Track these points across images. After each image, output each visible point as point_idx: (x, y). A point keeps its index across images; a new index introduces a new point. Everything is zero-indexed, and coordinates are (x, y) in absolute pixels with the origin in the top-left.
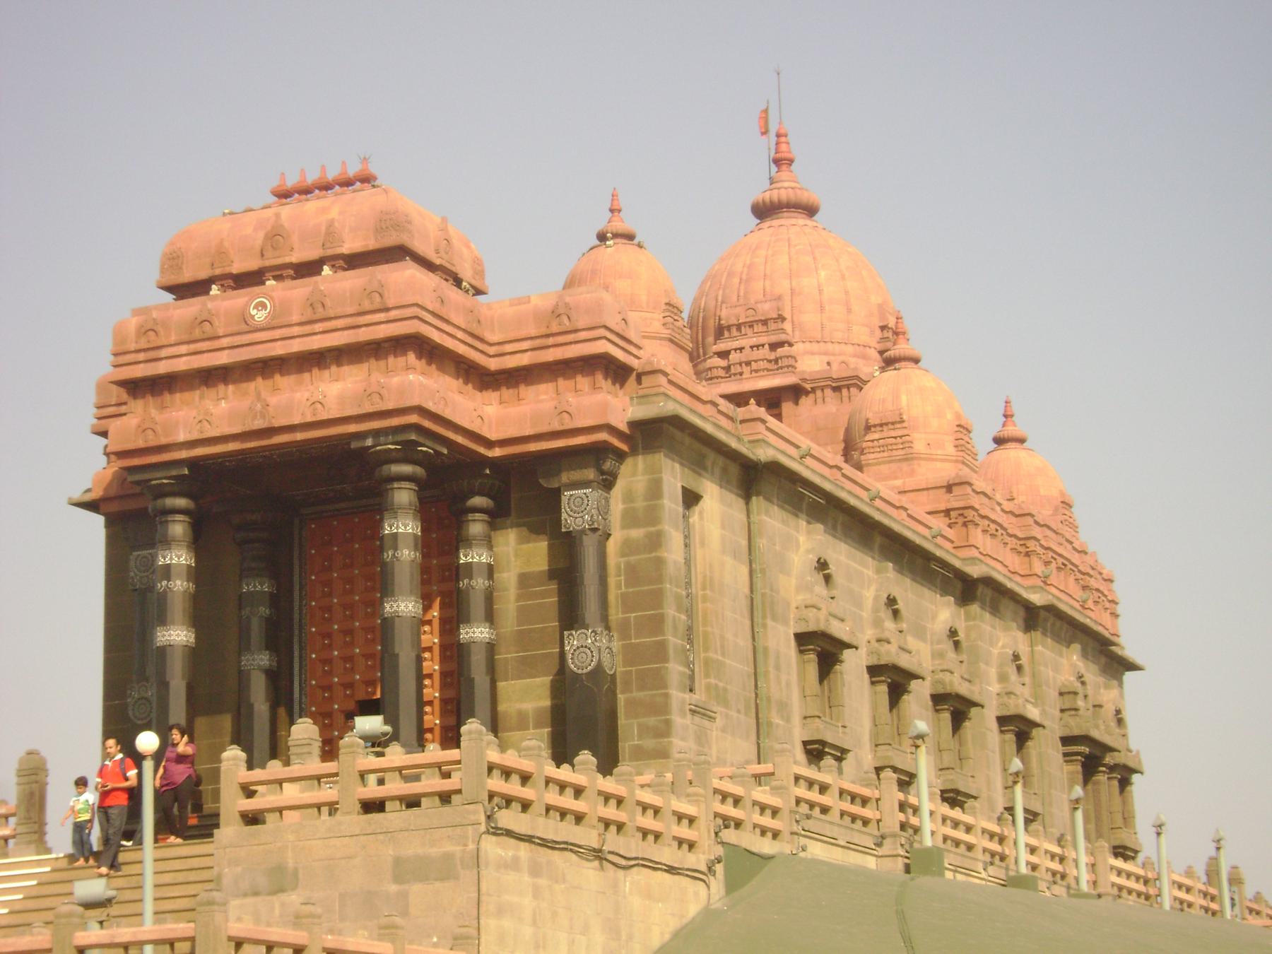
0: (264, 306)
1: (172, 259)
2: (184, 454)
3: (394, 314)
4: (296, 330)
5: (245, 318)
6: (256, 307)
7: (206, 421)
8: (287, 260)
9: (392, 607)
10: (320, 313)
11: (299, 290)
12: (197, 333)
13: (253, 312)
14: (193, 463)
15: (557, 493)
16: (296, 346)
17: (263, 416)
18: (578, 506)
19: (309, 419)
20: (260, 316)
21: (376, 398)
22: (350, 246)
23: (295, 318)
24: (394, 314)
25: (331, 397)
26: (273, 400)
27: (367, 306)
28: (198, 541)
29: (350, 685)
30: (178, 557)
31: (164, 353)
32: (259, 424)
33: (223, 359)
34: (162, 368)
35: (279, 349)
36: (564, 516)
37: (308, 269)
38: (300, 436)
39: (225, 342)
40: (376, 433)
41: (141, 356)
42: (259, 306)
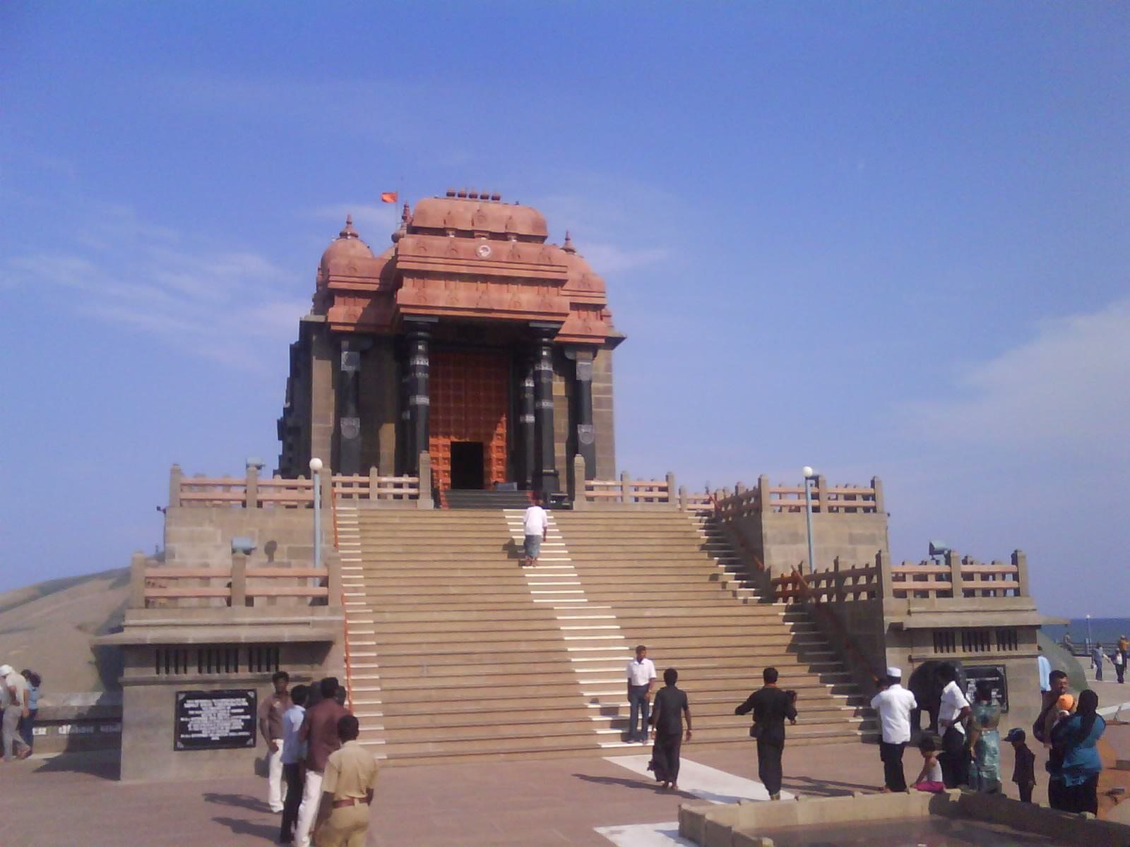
2: (440, 312)
3: (554, 269)
5: (476, 253)
6: (484, 249)
8: (489, 230)
11: (505, 247)
13: (481, 251)
15: (574, 363)
16: (505, 273)
19: (512, 309)
20: (484, 254)
24: (554, 269)
25: (524, 301)
28: (429, 354)
30: (422, 362)
33: (464, 270)
34: (429, 267)
35: (495, 272)
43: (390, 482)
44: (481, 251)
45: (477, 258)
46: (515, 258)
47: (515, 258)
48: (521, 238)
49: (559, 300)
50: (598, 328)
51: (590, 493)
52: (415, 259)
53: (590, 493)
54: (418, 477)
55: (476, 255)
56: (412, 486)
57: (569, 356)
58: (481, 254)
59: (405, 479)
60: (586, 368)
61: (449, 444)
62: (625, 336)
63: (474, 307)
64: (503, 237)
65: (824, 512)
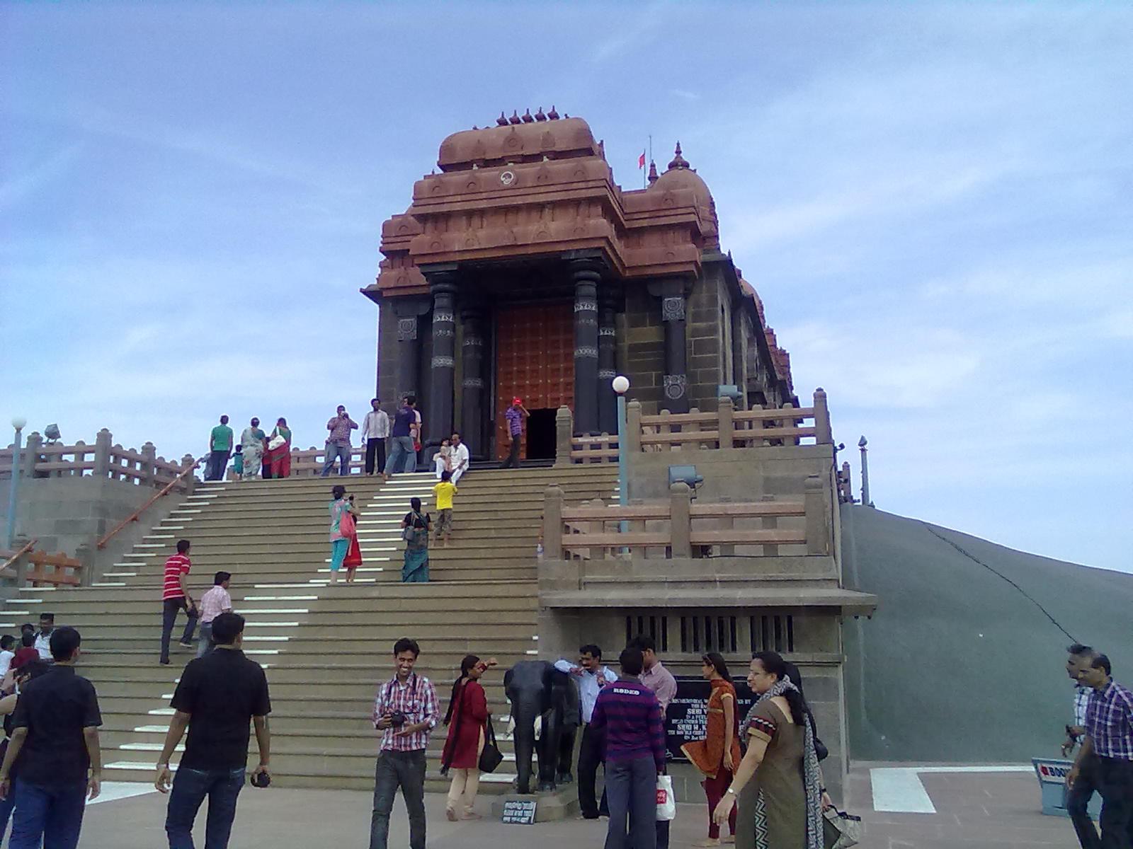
0: (510, 177)
1: (446, 149)
2: (458, 257)
3: (591, 184)
4: (532, 190)
7: (468, 240)
11: (530, 169)
13: (503, 179)
14: (462, 264)
15: (660, 299)
18: (673, 306)
22: (560, 146)
23: (530, 184)
24: (591, 184)
34: (445, 208)
37: (536, 158)
38: (530, 251)
39: (484, 195)
41: (432, 201)
42: (506, 176)
46: (543, 179)
47: (543, 179)
48: (557, 155)
51: (578, 454)
52: (432, 201)
53: (578, 454)
55: (498, 185)
57: (654, 290)
64: (536, 158)
65: (727, 451)
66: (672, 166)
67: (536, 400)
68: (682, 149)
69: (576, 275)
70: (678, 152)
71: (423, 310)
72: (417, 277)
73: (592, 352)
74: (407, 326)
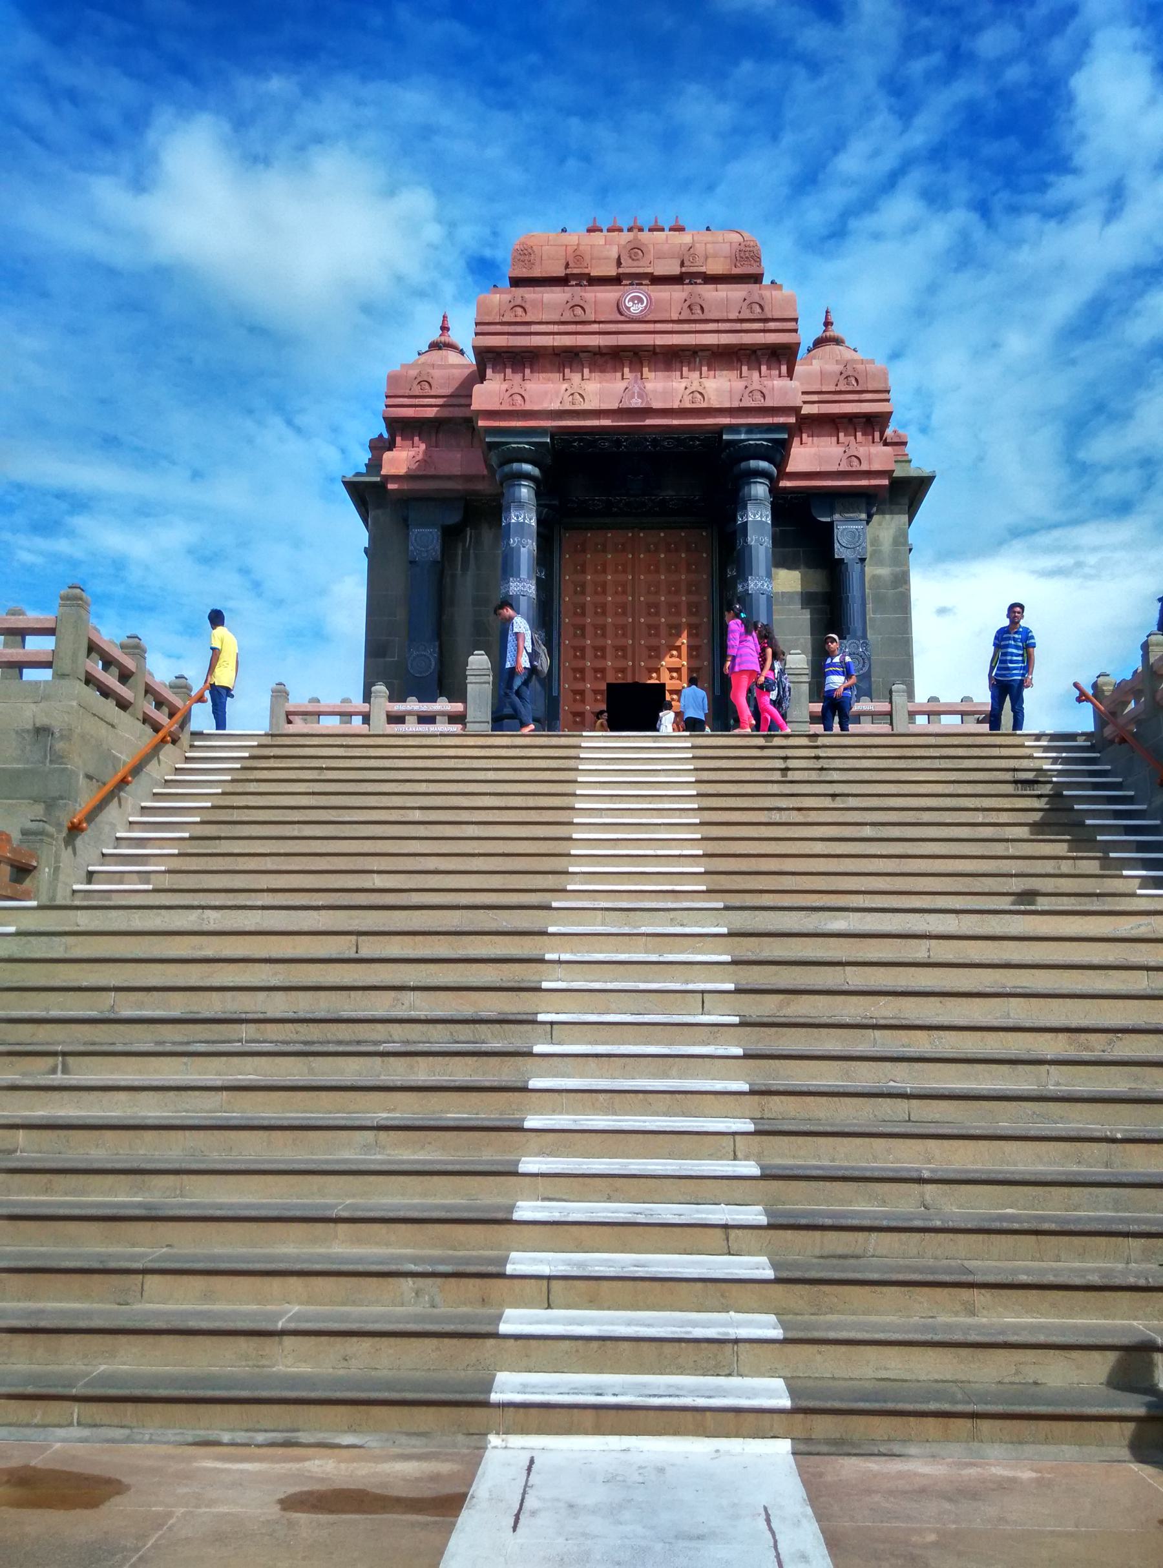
3: (772, 325)
6: (632, 300)
9: (756, 585)
10: (698, 315)
12: (568, 316)
13: (630, 304)
14: (556, 434)
15: (830, 526)
17: (640, 396)
19: (688, 405)
20: (635, 309)
21: (758, 396)
24: (772, 325)
26: (649, 386)
27: (746, 314)
29: (603, 671)
31: (534, 328)
32: (636, 403)
36: (836, 545)
40: (751, 429)
43: (410, 713)
44: (630, 304)
45: (622, 318)
49: (782, 389)
50: (874, 456)
54: (462, 698)
55: (621, 314)
56: (457, 718)
58: (628, 308)
59: (442, 705)
60: (849, 534)
61: (604, 687)
62: (926, 471)
63: (615, 406)
66: (819, 343)
67: (623, 670)
68: (832, 318)
69: (743, 465)
70: (827, 324)
71: (454, 518)
72: (457, 461)
73: (756, 585)
74: (426, 540)
